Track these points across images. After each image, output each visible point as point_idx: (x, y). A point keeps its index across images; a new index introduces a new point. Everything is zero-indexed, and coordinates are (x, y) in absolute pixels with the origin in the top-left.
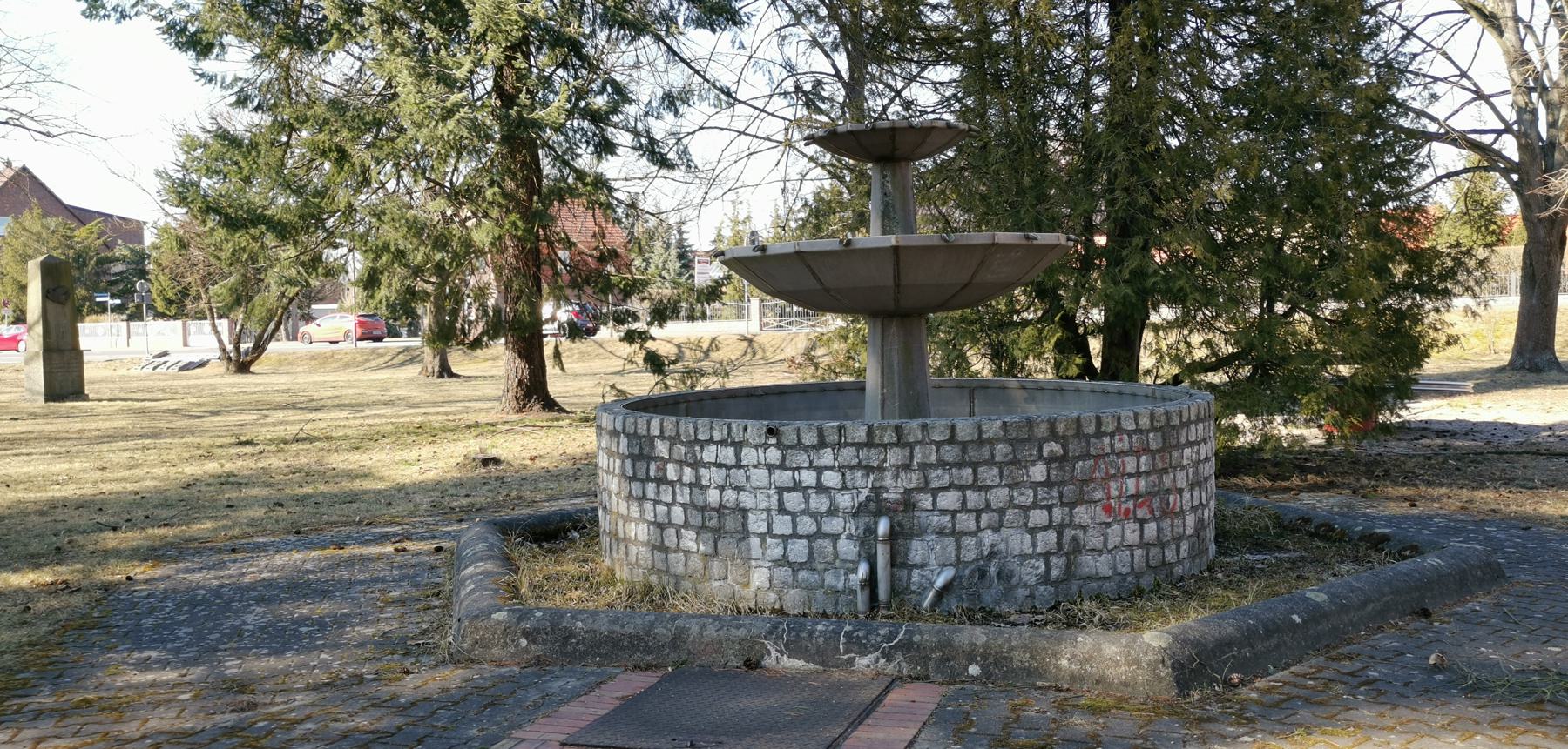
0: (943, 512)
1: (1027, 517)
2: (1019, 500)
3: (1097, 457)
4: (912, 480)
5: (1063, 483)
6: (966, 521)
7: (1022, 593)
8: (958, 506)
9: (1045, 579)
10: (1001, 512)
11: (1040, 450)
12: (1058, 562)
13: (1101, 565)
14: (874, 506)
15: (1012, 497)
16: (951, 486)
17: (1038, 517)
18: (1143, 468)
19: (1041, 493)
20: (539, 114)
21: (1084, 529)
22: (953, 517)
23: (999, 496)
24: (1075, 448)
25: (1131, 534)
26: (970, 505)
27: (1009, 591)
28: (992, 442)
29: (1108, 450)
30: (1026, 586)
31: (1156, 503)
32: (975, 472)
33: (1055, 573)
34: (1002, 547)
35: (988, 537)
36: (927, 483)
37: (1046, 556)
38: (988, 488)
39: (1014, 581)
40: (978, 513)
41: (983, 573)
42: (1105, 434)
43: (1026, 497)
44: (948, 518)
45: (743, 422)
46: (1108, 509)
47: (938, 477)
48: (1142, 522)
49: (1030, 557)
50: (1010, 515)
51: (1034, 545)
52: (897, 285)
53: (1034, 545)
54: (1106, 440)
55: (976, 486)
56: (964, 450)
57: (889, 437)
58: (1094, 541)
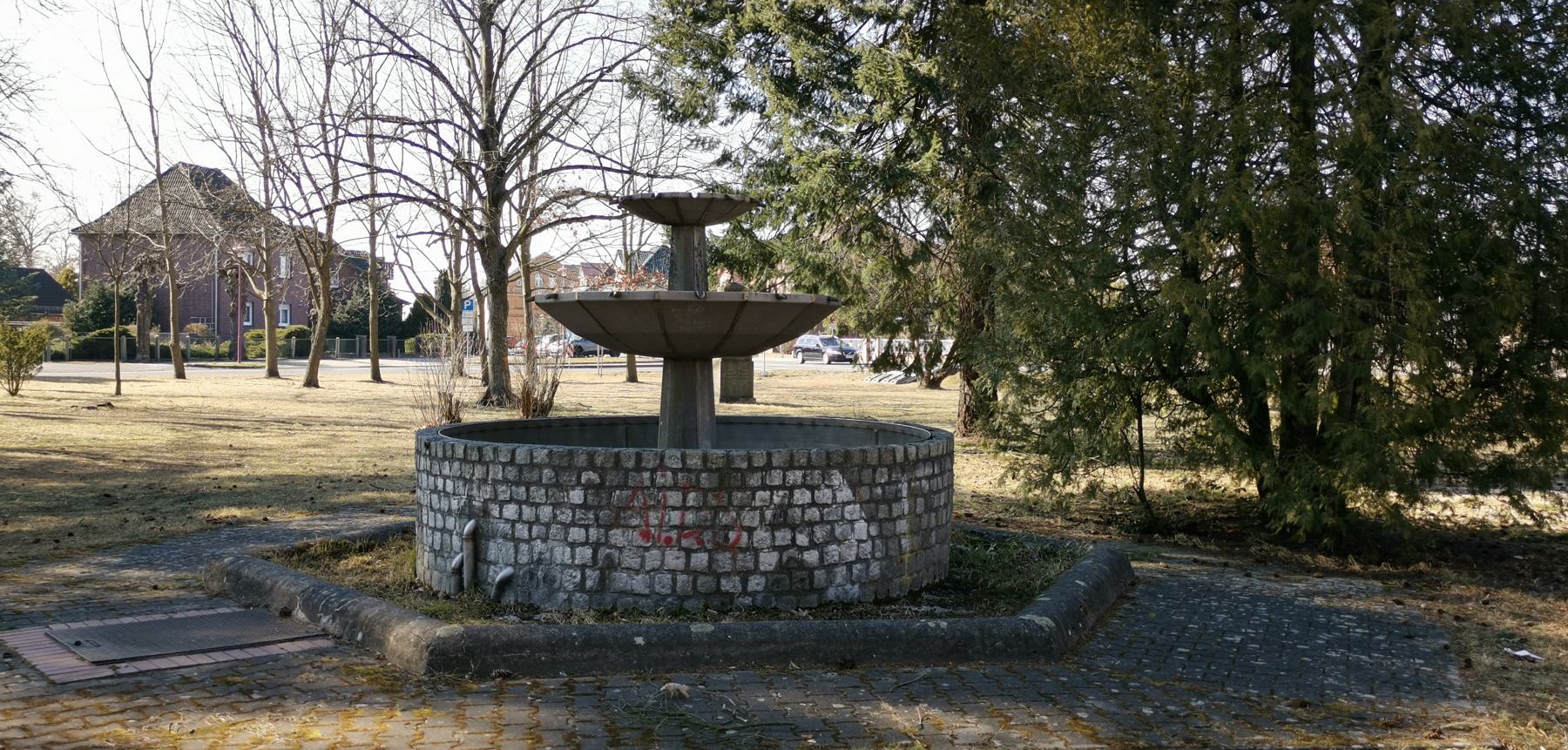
0: (507, 520)
1: (567, 533)
2: (561, 518)
3: (635, 489)
4: (487, 492)
5: (599, 507)
6: (522, 531)
7: (562, 596)
8: (516, 517)
9: (581, 587)
10: (548, 525)
11: (579, 477)
12: (592, 578)
13: (638, 583)
14: (467, 512)
15: (555, 516)
16: (511, 500)
17: (576, 534)
18: (691, 503)
19: (579, 514)
20: (912, 165)
21: (621, 549)
22: (513, 526)
23: (546, 512)
24: (612, 478)
25: (674, 559)
26: (525, 517)
27: (552, 593)
28: (540, 467)
29: (647, 483)
30: (566, 591)
31: (707, 536)
32: (528, 490)
33: (589, 583)
34: (547, 555)
35: (539, 546)
36: (496, 495)
37: (583, 567)
38: (537, 505)
39: (556, 585)
40: (531, 524)
41: (532, 575)
42: (646, 469)
43: (565, 516)
44: (509, 526)
45: (511, 446)
46: (646, 535)
47: (504, 492)
48: (689, 552)
49: (569, 567)
50: (554, 529)
51: (573, 557)
52: (666, 335)
53: (573, 557)
54: (646, 475)
55: (528, 502)
56: (520, 471)
57: (474, 456)
58: (631, 560)
